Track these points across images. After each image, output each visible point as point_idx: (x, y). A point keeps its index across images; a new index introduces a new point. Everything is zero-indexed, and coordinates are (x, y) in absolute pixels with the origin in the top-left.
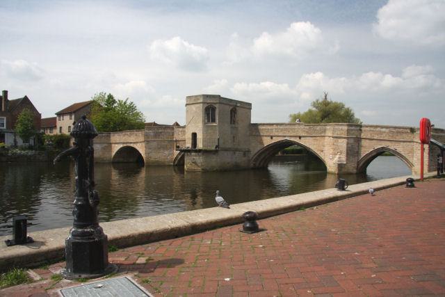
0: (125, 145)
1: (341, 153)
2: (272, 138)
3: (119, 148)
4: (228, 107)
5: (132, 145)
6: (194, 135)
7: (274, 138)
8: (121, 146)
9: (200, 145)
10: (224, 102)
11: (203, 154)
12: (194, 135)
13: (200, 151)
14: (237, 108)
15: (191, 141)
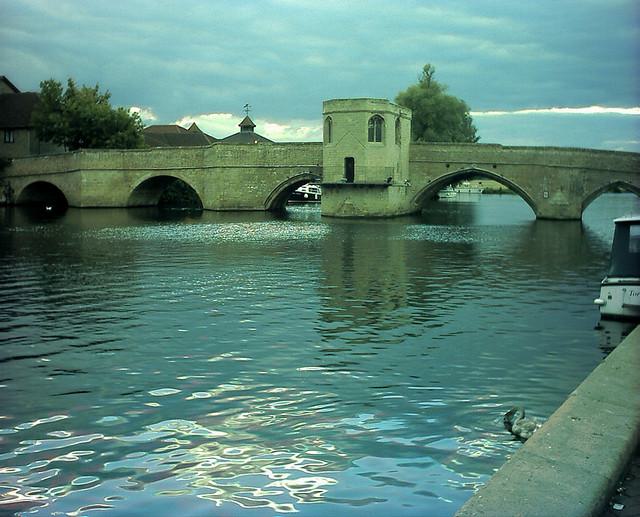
0: (158, 174)
1: (562, 189)
2: (448, 166)
3: (143, 179)
6: (350, 162)
8: (149, 175)
9: (359, 178)
12: (350, 162)
15: (343, 171)
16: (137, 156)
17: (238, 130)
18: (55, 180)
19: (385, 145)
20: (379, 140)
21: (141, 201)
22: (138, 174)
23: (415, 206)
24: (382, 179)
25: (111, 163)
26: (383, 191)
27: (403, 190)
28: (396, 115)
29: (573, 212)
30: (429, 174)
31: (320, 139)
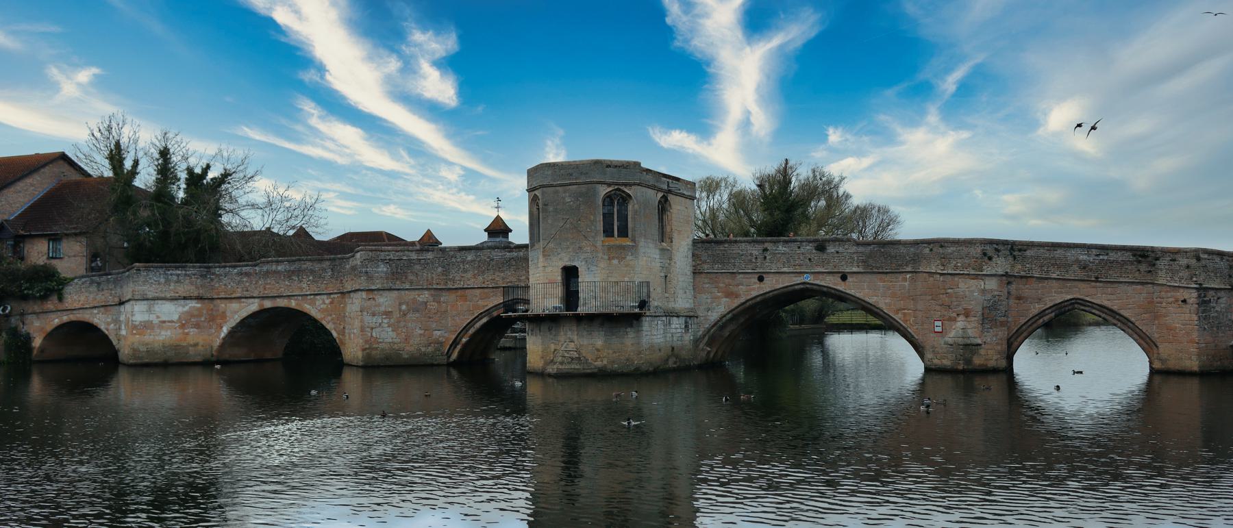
0: (268, 304)
1: (967, 316)
2: (761, 279)
3: (244, 314)
4: (651, 192)
5: (293, 304)
6: (570, 274)
7: (767, 279)
8: (254, 306)
10: (650, 179)
11: (602, 325)
12: (570, 274)
13: (591, 318)
14: (670, 197)
15: (559, 291)
16: (228, 278)
17: (484, 237)
18: (100, 320)
19: (634, 240)
20: (623, 232)
21: (239, 353)
22: (235, 305)
23: (704, 352)
24: (629, 304)
25: (186, 288)
26: (631, 326)
27: (677, 323)
28: (660, 190)
29: (989, 356)
30: (730, 295)
31: (526, 241)
